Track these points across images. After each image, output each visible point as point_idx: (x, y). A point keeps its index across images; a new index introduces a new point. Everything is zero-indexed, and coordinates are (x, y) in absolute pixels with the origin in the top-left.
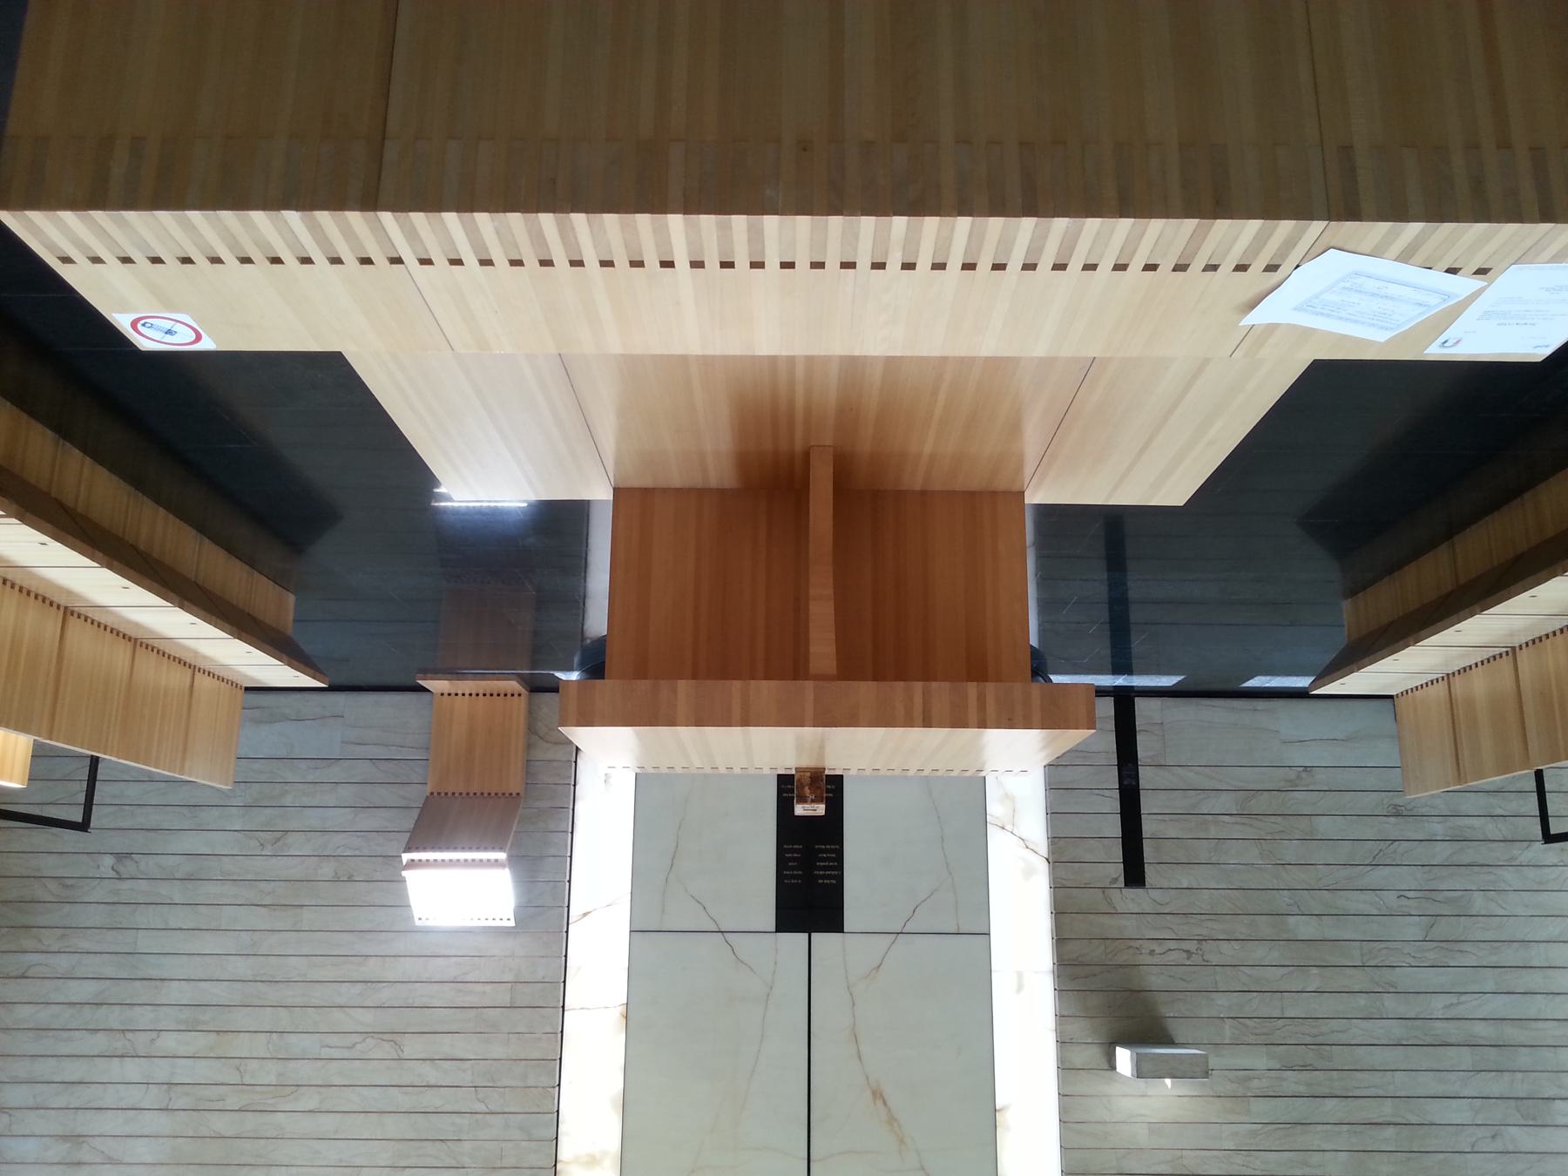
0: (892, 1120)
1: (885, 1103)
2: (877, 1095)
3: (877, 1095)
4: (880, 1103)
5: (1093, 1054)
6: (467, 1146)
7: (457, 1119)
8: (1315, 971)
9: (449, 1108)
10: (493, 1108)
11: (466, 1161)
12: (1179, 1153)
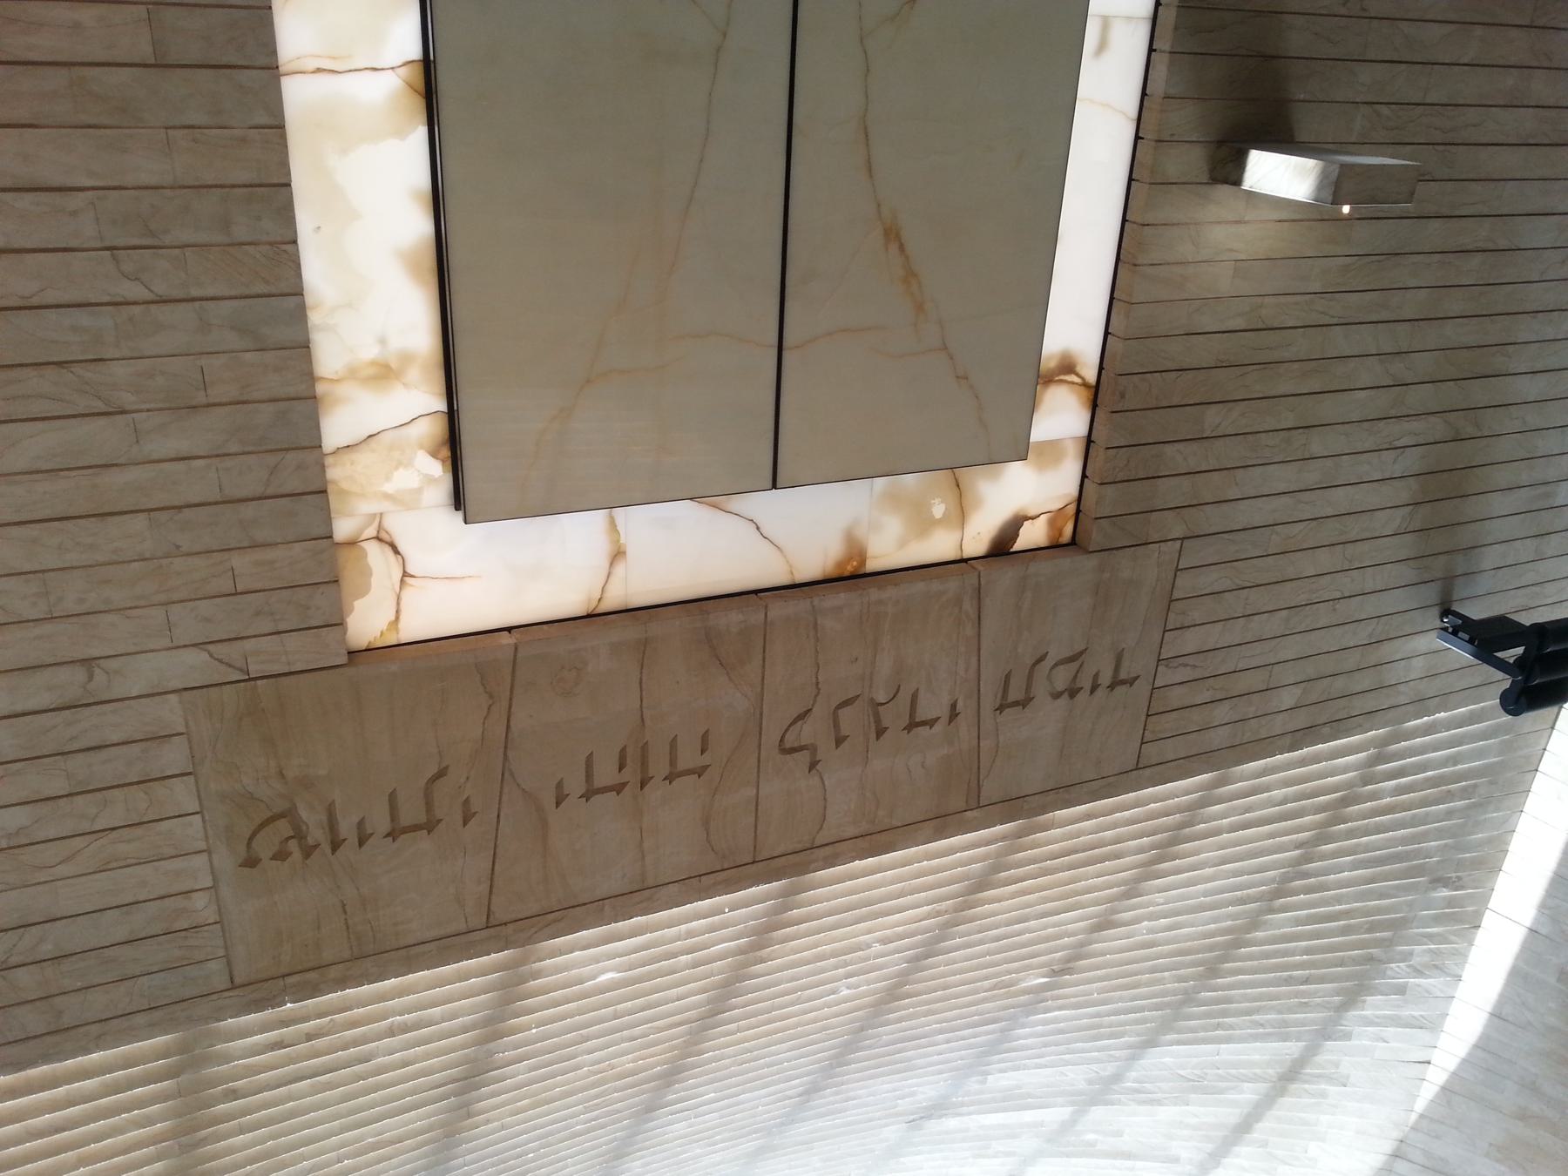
0: (910, 275)
1: (902, 248)
2: (892, 235)
3: (892, 235)
4: (894, 247)
5: (1189, 160)
6: (120, 371)
7: (83, 318)
8: (1479, 31)
9: (50, 297)
10: (161, 289)
11: (128, 399)
12: (1259, 300)
